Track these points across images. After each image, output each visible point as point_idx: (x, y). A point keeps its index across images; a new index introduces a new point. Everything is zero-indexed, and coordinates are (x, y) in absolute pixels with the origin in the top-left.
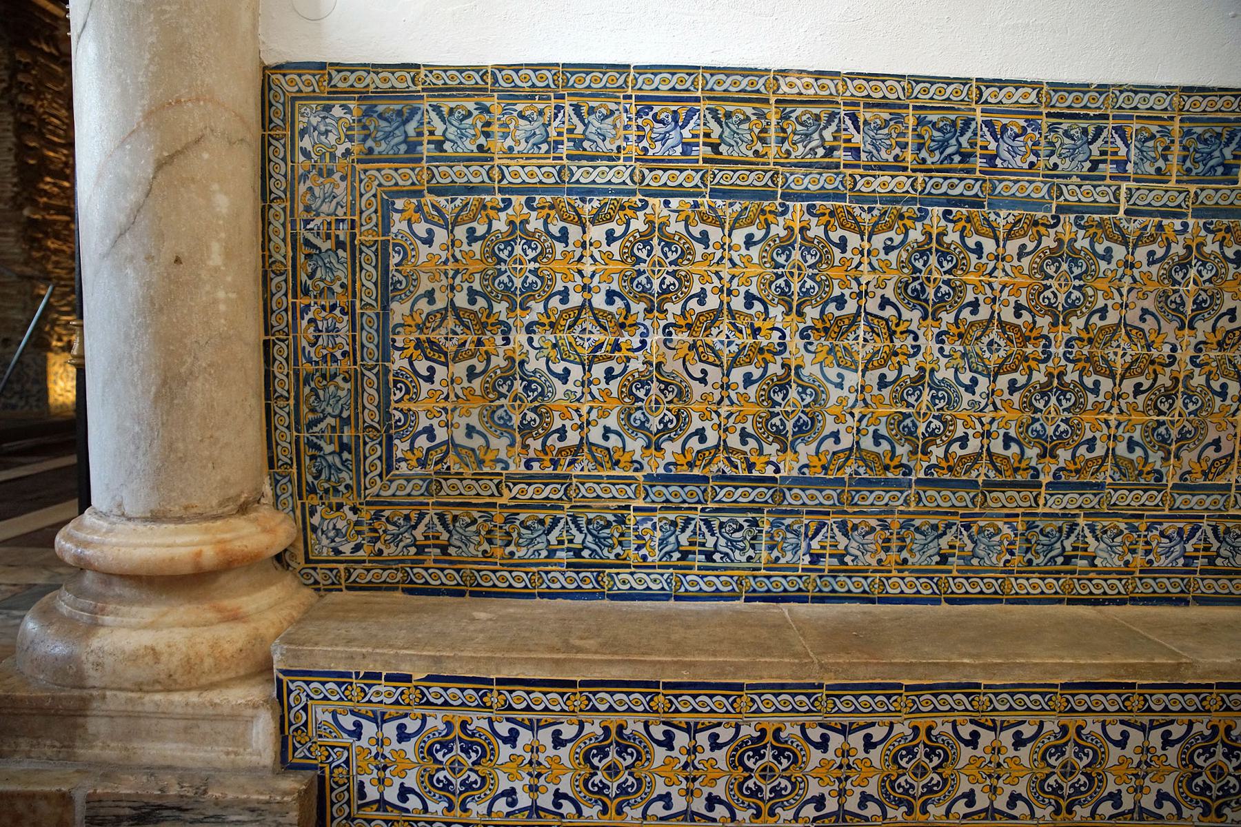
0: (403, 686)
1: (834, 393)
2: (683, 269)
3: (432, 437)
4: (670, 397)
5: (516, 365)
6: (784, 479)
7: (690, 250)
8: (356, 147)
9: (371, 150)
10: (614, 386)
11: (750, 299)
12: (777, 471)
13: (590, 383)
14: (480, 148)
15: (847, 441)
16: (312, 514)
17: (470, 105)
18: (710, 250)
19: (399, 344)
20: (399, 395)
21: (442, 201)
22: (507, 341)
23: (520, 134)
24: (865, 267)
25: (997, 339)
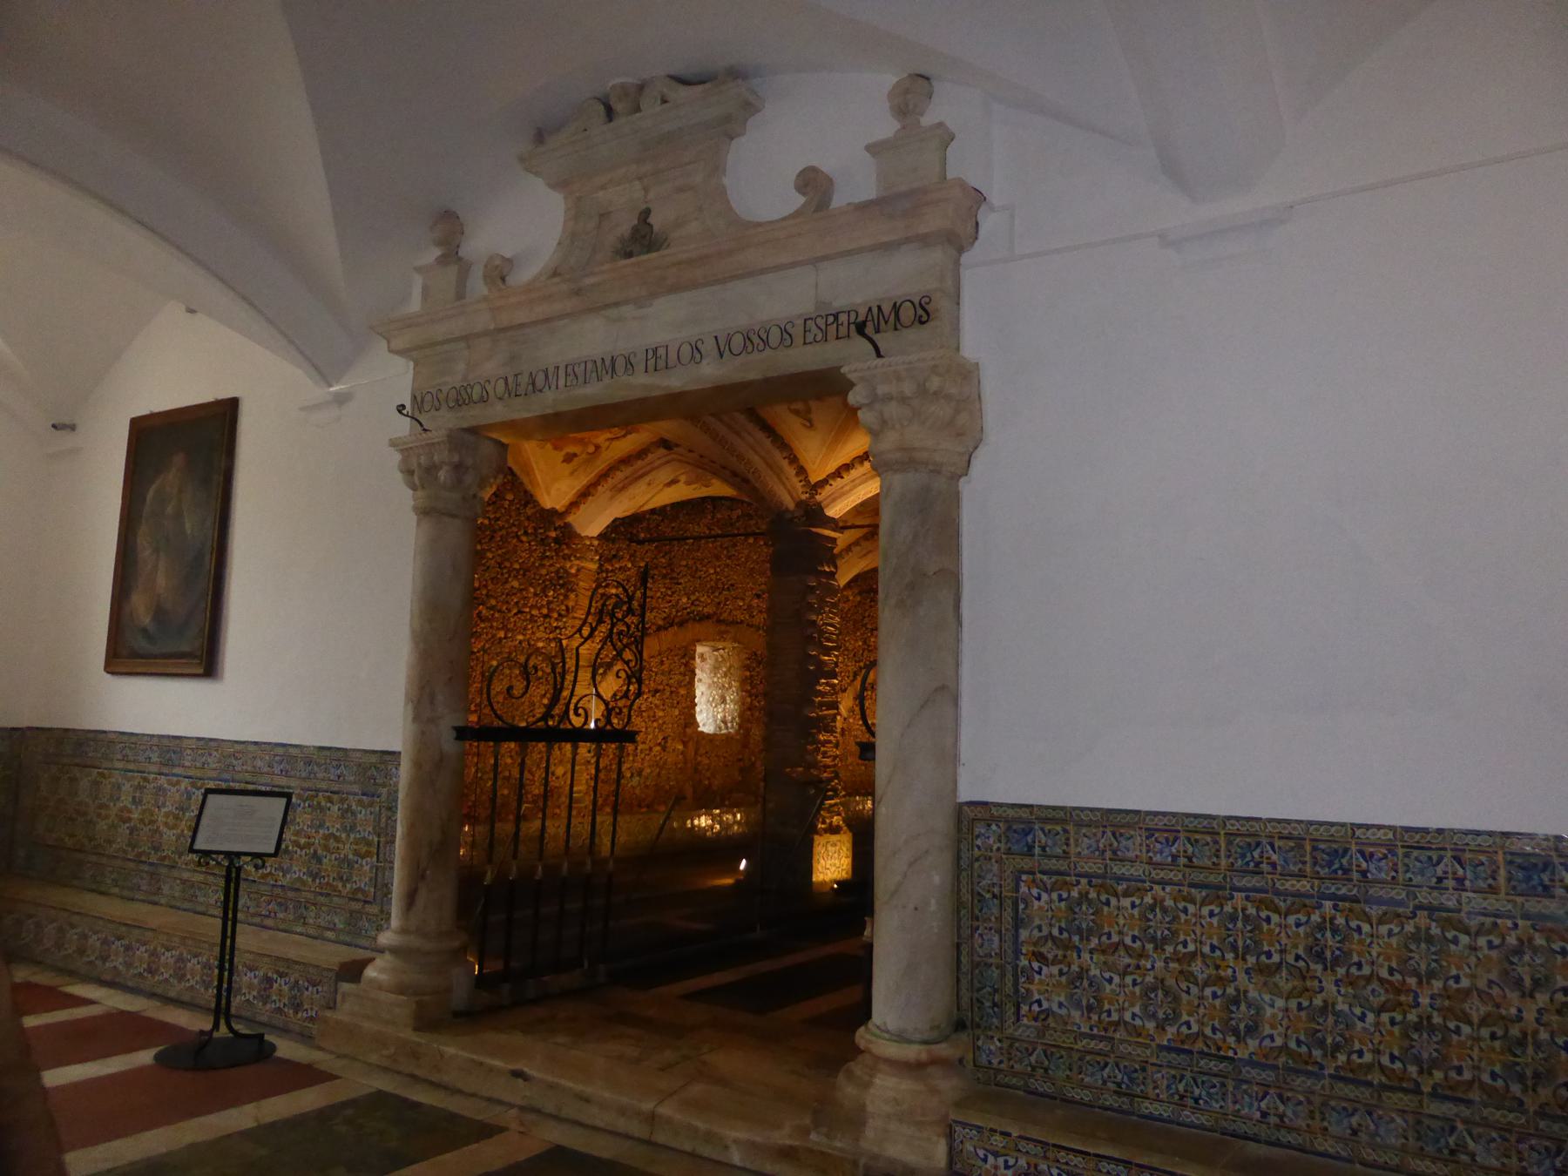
0: (1008, 1139)
1: (1269, 1012)
2: (1175, 926)
3: (1040, 1005)
4: (1169, 999)
5: (1083, 971)
6: (1240, 1059)
7: (1179, 918)
8: (1002, 846)
9: (1010, 849)
10: (1137, 989)
11: (1213, 948)
12: (1236, 1053)
13: (1124, 986)
14: (1064, 852)
15: (1279, 1042)
16: (978, 1039)
17: (1059, 828)
18: (1189, 917)
19: (1024, 951)
20: (1023, 980)
21: (1045, 878)
22: (1079, 957)
23: (1084, 846)
24: (1283, 934)
25: (1377, 988)
